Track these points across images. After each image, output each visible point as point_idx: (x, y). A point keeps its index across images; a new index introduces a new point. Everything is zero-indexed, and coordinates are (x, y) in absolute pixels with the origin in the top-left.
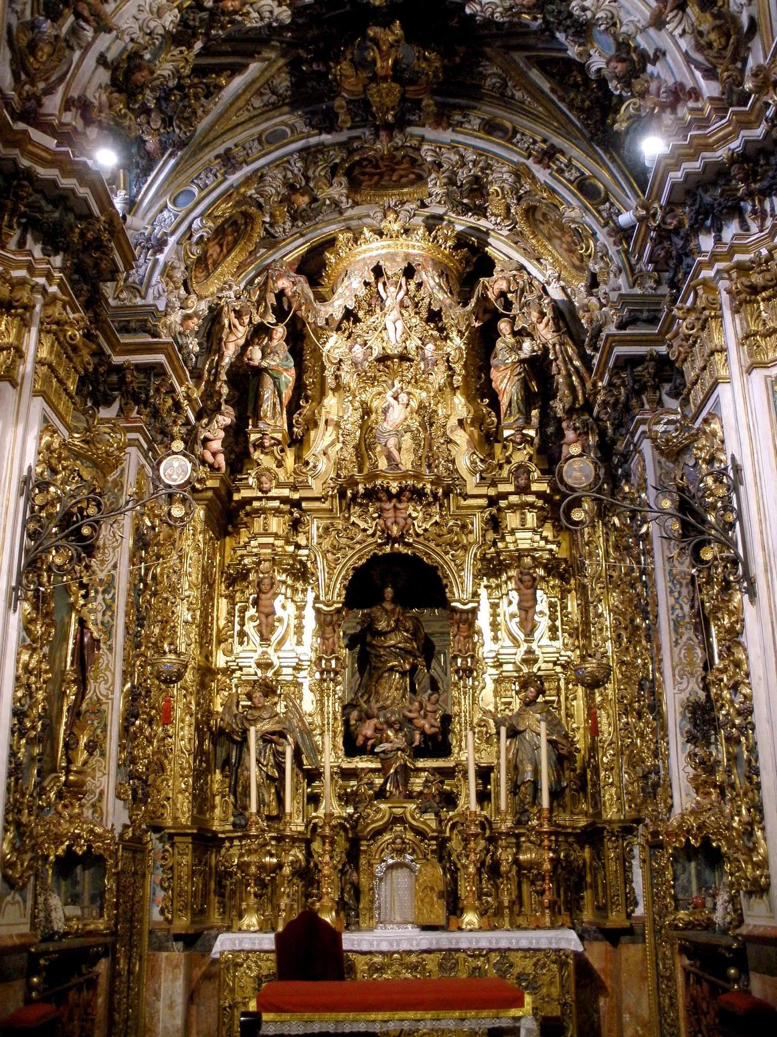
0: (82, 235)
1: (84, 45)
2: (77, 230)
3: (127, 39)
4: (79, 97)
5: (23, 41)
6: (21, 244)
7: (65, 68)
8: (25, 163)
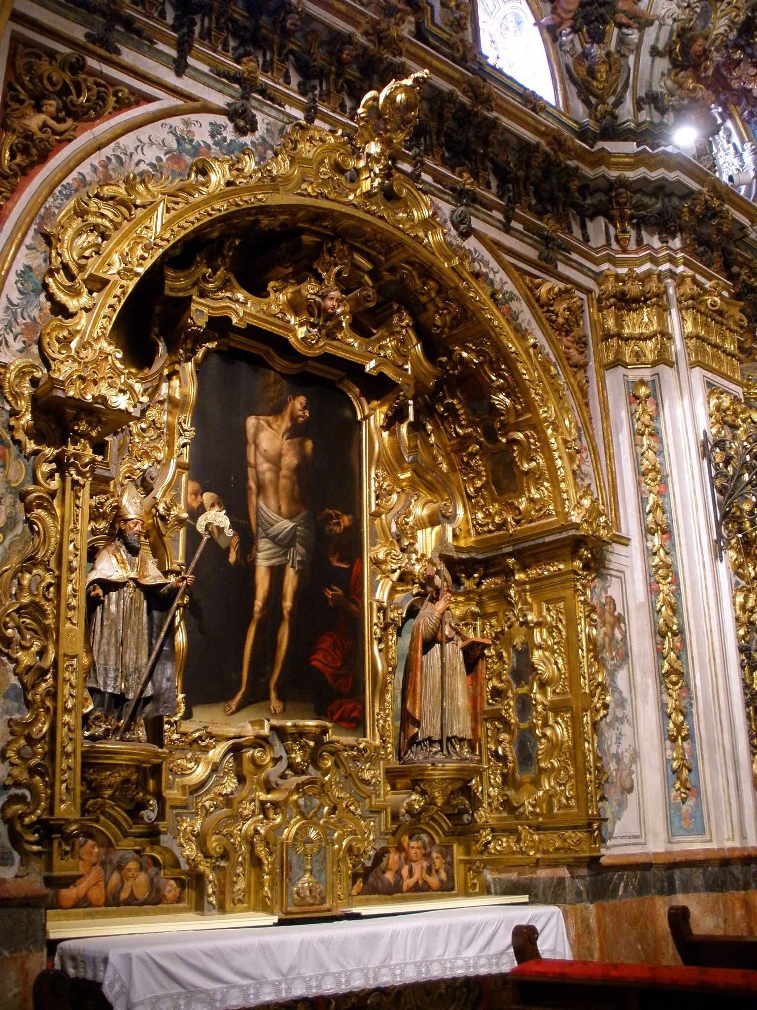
0: (692, 211)
1: (633, 47)
2: (685, 210)
3: (670, 21)
4: (647, 95)
5: (582, 71)
6: (639, 241)
7: (625, 75)
8: (614, 174)
